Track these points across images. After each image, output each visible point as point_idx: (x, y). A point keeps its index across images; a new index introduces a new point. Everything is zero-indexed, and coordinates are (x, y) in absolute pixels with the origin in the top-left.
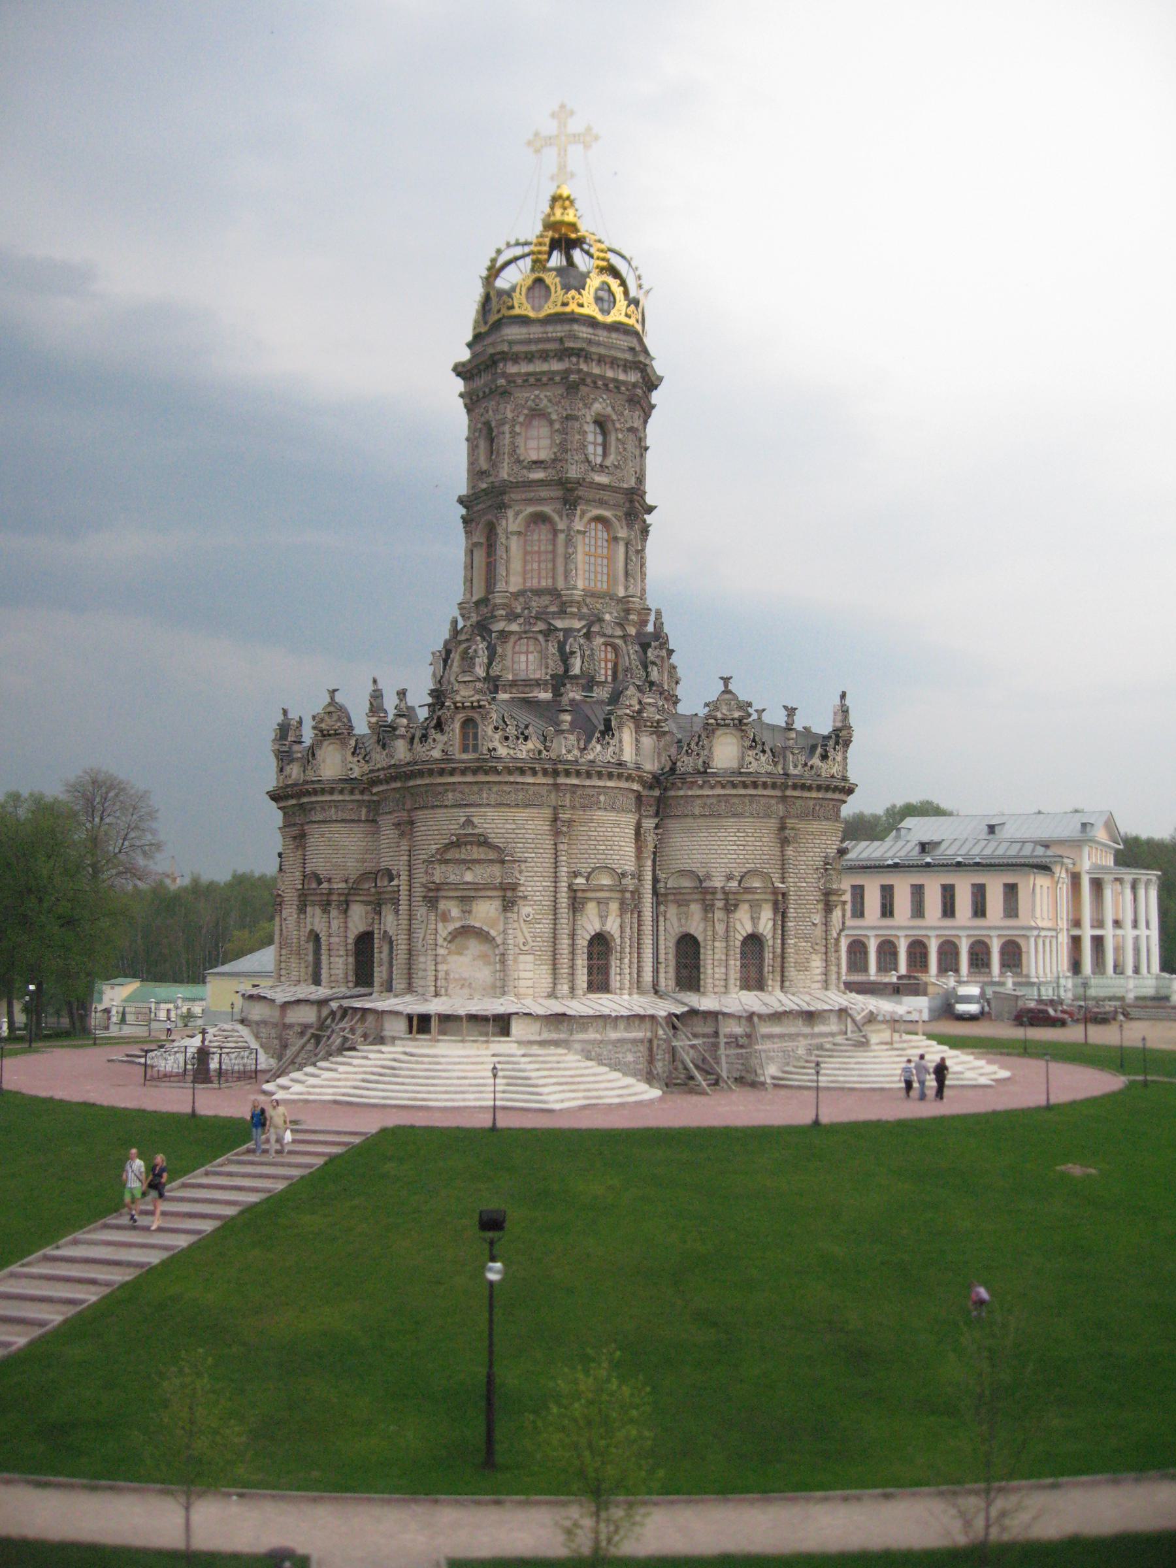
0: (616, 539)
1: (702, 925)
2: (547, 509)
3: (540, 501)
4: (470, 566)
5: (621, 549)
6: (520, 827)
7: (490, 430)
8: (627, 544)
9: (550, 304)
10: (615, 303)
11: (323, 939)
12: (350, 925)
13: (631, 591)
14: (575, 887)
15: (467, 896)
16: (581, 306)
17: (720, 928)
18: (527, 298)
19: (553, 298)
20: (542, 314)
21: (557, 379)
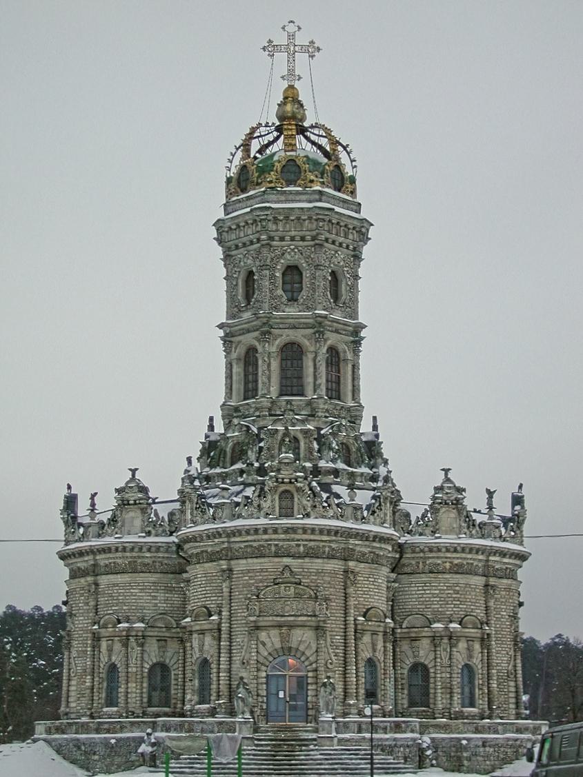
4: (229, 376)
7: (251, 273)
11: (121, 669)
12: (146, 656)
14: (357, 622)
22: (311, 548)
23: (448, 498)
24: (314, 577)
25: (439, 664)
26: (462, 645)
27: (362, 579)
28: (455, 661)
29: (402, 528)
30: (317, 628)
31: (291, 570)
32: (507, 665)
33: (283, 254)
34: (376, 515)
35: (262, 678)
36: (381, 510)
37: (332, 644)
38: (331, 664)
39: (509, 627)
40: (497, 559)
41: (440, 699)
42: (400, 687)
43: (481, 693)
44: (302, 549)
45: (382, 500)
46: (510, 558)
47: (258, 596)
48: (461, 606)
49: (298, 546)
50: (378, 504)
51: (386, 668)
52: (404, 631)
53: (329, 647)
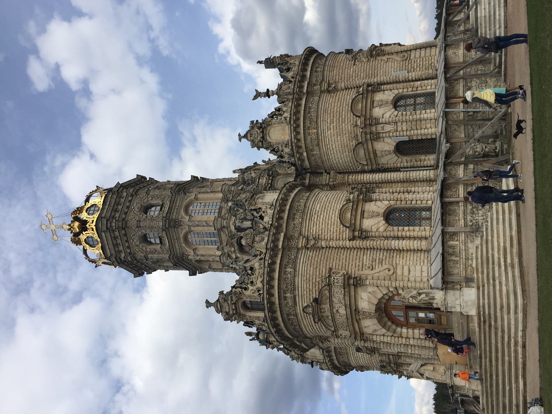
0: (196, 199)
1: (387, 140)
2: (182, 236)
3: (178, 239)
5: (200, 196)
6: (307, 274)
8: (199, 193)
9: (94, 236)
10: (96, 205)
13: (219, 189)
15: (355, 313)
16: (93, 221)
17: (388, 128)
18: (94, 247)
19: (92, 235)
20: (99, 240)
21: (123, 232)
22: (286, 287)
23: (258, 134)
24: (311, 285)
25: (394, 134)
26: (377, 112)
27: (315, 229)
28: (390, 119)
29: (288, 168)
30: (355, 286)
31: (306, 307)
32: (396, 62)
33: (137, 246)
34: (263, 215)
35: (407, 332)
36: (260, 208)
37: (371, 268)
38: (389, 270)
39: (363, 64)
40: (306, 84)
41: (426, 130)
42: (419, 163)
43: (420, 88)
44: (288, 295)
45: (253, 208)
46: (306, 70)
47: (334, 332)
48: (343, 117)
49: (285, 298)
50: (255, 214)
51: (395, 199)
52: (369, 163)
53: (373, 272)
